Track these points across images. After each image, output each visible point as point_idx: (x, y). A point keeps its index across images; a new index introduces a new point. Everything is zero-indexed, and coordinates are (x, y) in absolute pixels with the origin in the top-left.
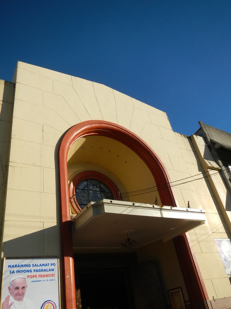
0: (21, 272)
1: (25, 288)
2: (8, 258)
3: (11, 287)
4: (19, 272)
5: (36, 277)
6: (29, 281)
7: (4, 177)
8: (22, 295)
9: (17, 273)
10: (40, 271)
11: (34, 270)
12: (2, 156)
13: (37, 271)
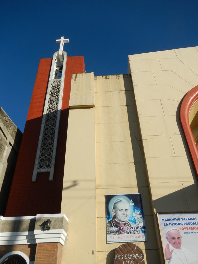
0: (173, 224)
1: (180, 238)
2: (160, 213)
3: (168, 237)
4: (171, 224)
5: (187, 229)
6: (182, 233)
7: (141, 149)
9: (170, 225)
10: (189, 224)
11: (184, 224)
12: (135, 133)
13: (187, 224)
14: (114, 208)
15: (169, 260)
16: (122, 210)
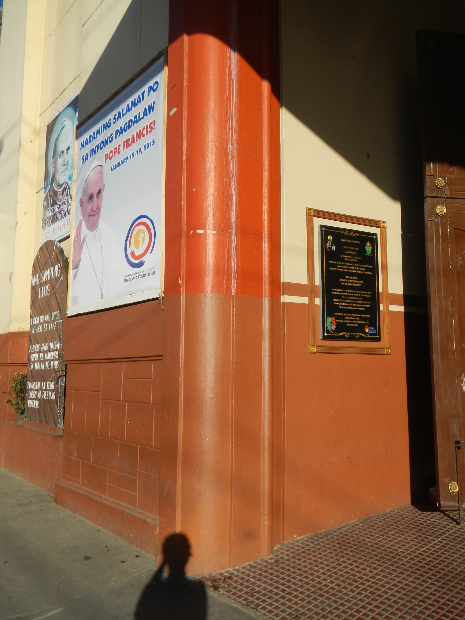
1: (102, 191)
4: (94, 151)
8: (96, 216)
14: (55, 152)
15: (76, 270)
16: (63, 152)
